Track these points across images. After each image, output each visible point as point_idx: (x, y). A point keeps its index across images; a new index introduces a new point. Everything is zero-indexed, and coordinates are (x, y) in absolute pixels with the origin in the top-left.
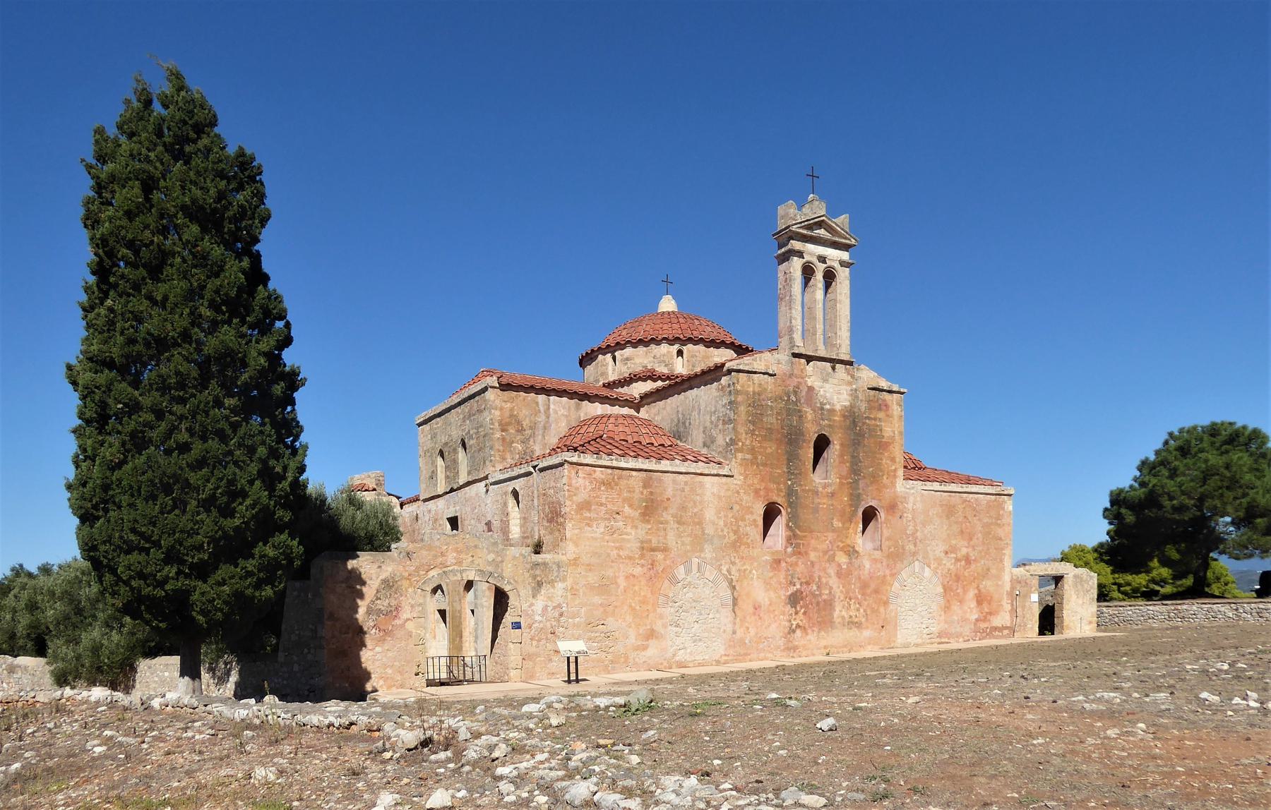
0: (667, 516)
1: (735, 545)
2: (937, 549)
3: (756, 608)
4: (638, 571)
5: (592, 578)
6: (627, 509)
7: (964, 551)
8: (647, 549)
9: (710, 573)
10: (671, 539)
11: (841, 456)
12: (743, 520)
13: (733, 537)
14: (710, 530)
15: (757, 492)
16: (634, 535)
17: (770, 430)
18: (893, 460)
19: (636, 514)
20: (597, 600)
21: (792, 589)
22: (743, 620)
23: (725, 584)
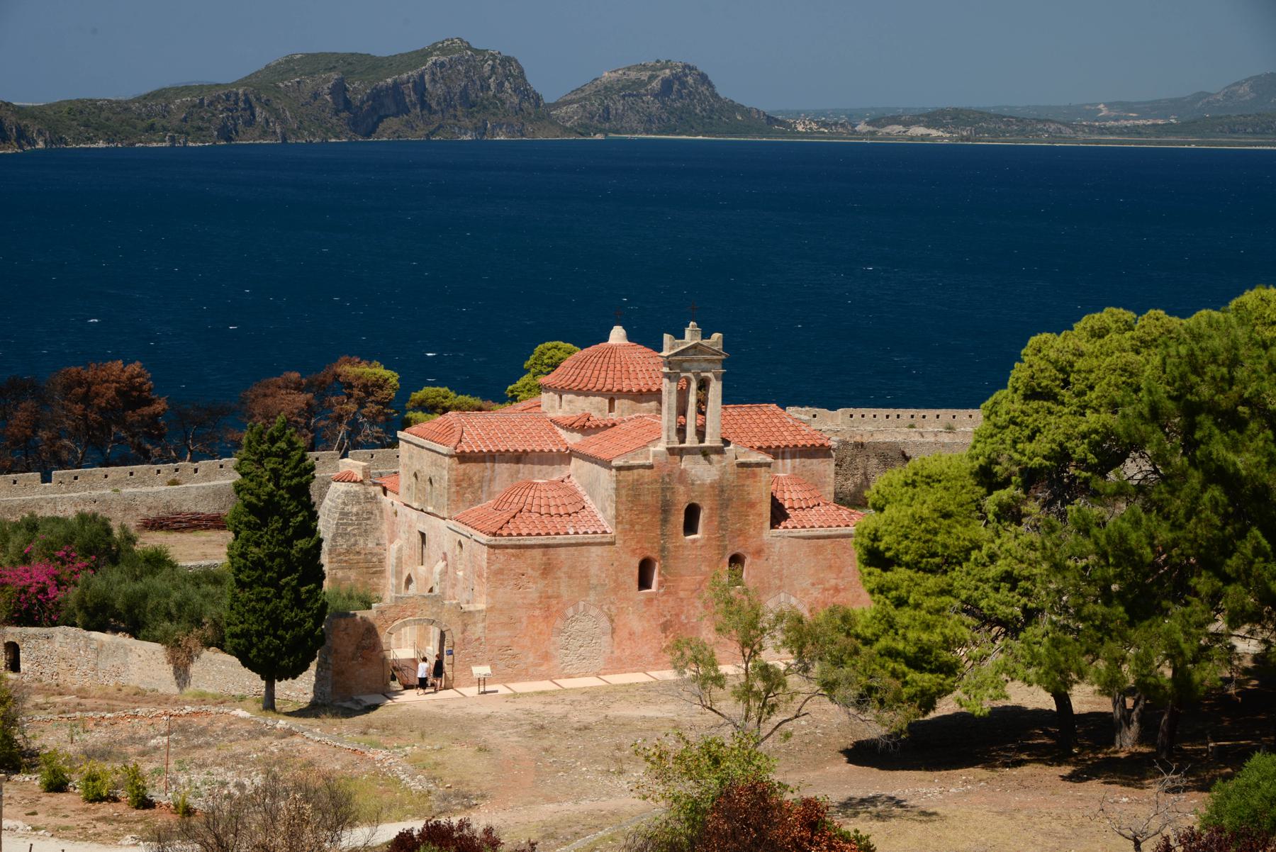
0: (560, 574)
1: (615, 590)
2: (807, 583)
3: (631, 634)
4: (537, 613)
5: (504, 619)
6: (530, 571)
7: (833, 582)
8: (545, 598)
9: (594, 612)
10: (564, 590)
11: (710, 517)
12: (621, 571)
13: (613, 585)
14: (594, 581)
15: (633, 551)
16: (533, 589)
17: (647, 506)
18: (760, 515)
19: (537, 574)
20: (507, 633)
21: (662, 620)
22: (620, 644)
23: (605, 618)
